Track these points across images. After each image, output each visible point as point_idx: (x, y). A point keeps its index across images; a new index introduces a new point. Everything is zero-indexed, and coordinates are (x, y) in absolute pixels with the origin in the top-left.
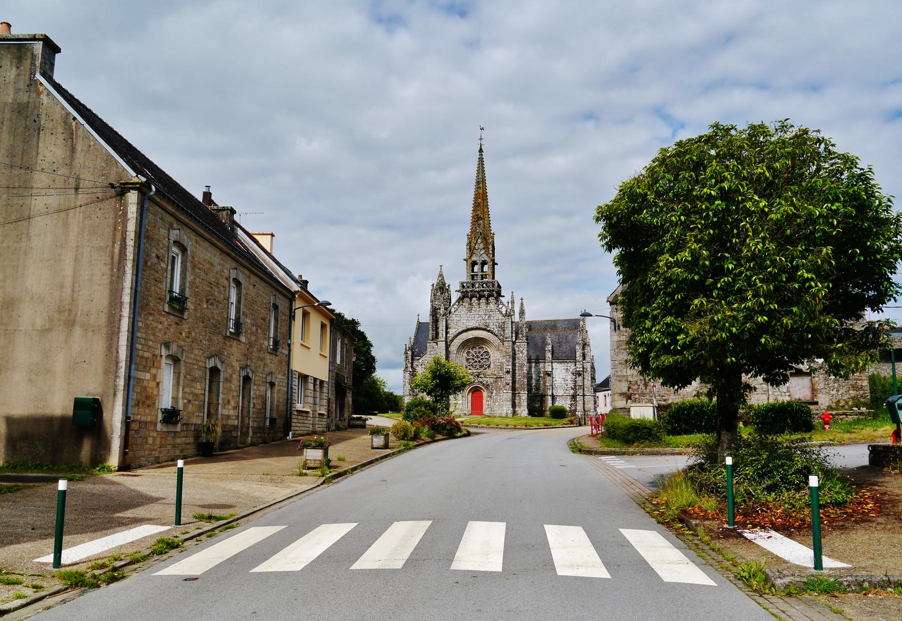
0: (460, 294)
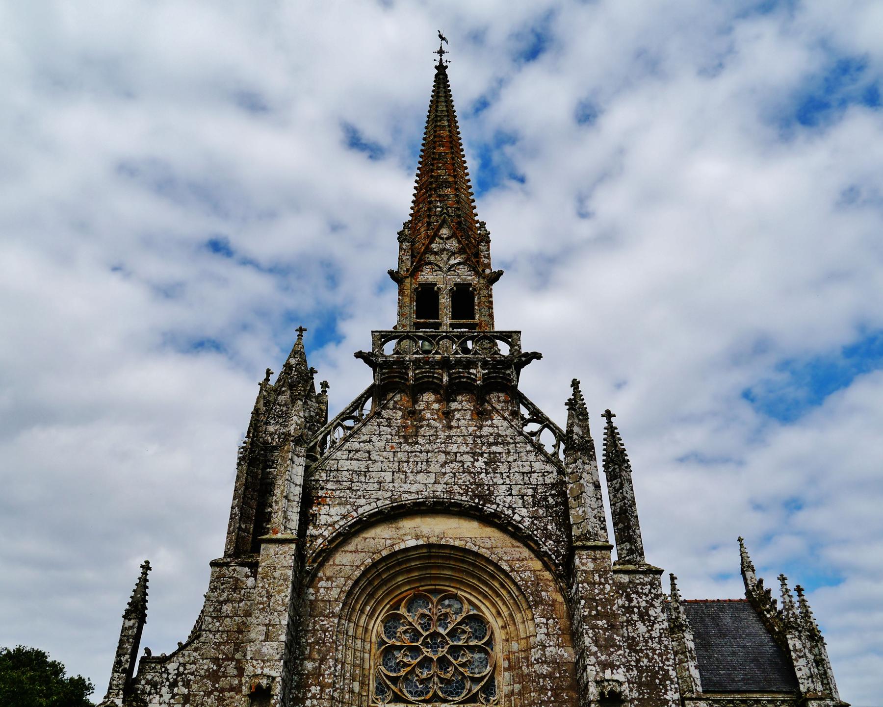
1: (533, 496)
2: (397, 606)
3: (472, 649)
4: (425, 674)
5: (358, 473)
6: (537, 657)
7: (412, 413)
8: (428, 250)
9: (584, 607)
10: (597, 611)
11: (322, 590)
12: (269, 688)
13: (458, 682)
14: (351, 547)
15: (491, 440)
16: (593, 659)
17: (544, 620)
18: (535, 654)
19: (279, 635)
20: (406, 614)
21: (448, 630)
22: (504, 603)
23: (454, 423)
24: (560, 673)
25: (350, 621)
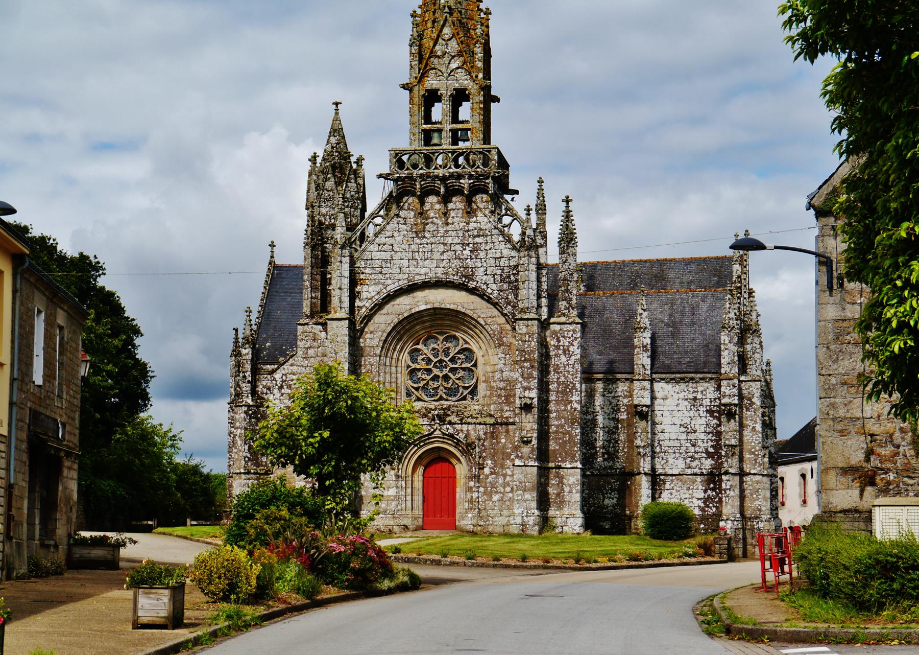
0: (390, 186)
1: (501, 275)
3: (464, 369)
4: (436, 384)
5: (386, 261)
7: (422, 214)
8: (432, 54)
14: (384, 311)
15: (475, 233)
16: (519, 385)
23: (450, 221)
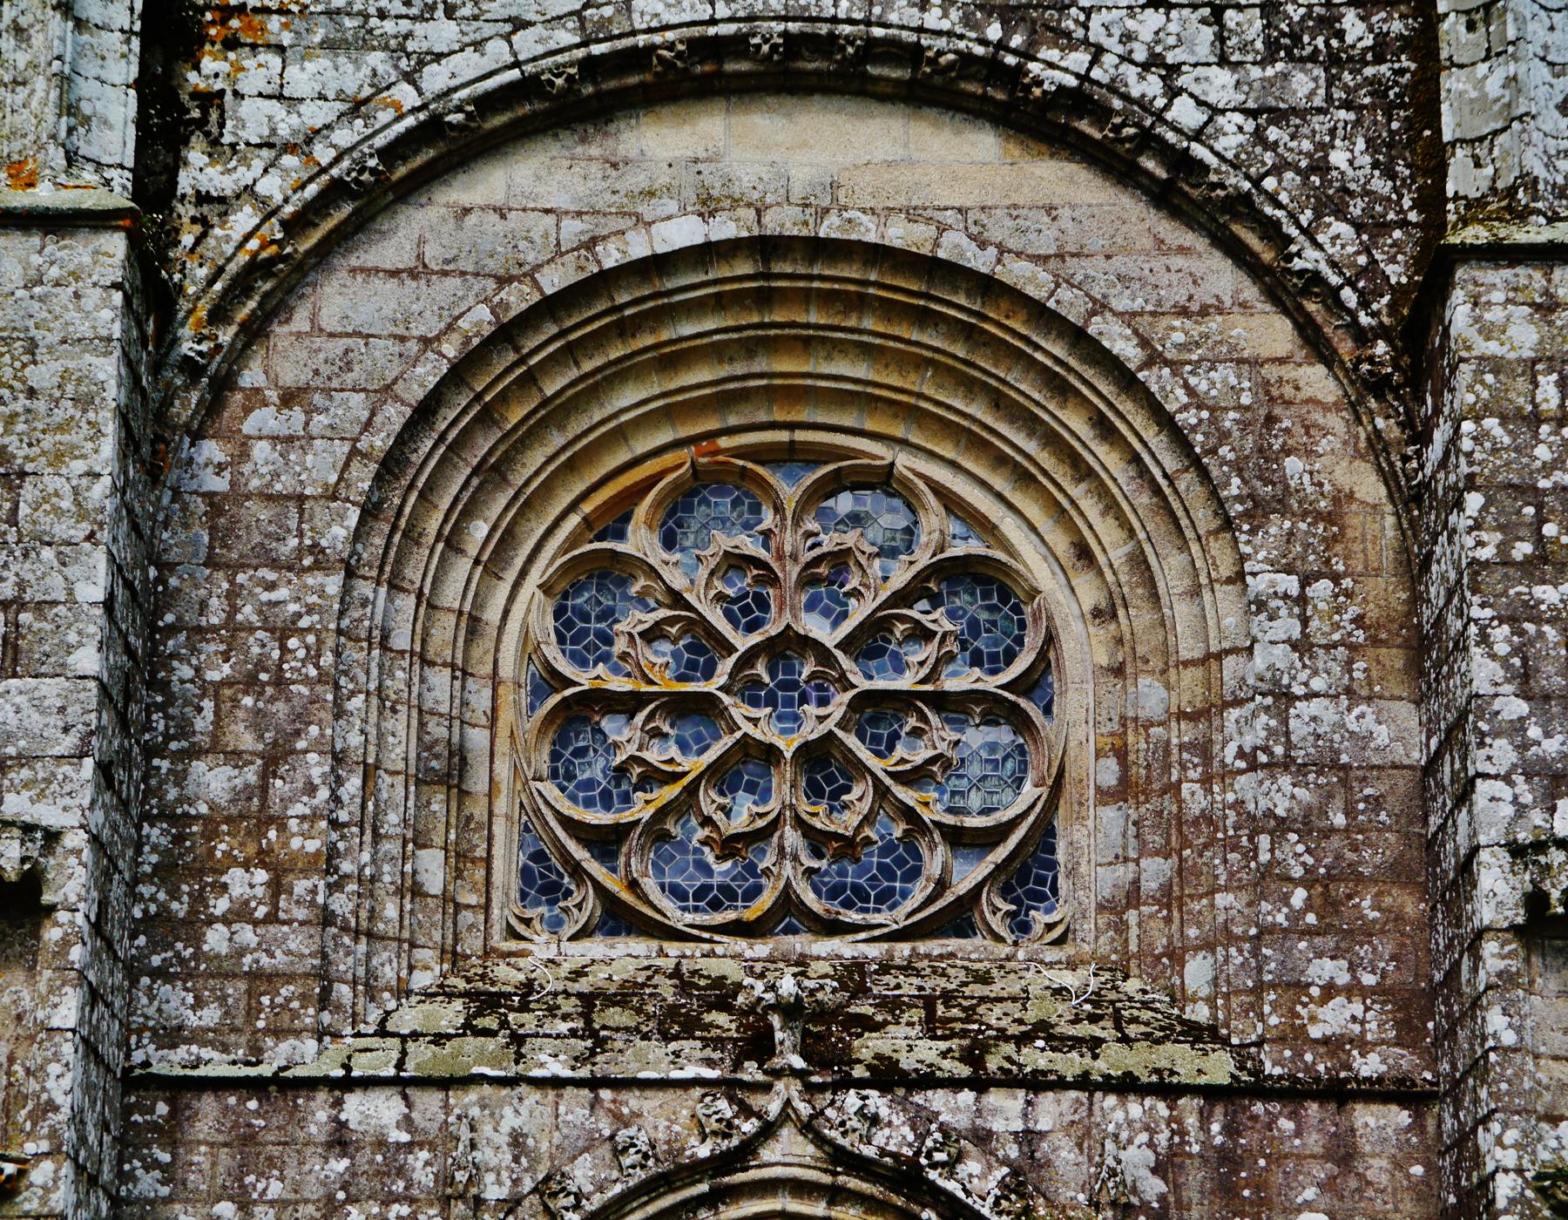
2: (614, 520)
3: (952, 706)
4: (743, 814)
6: (1248, 741)
9: (1477, 526)
10: (1539, 540)
11: (261, 450)
12: (33, 880)
13: (889, 848)
16: (1503, 753)
17: (1291, 584)
18: (1244, 730)
19: (69, 649)
20: (655, 554)
21: (846, 628)
22: (1111, 507)
24: (1350, 812)
25: (395, 587)
